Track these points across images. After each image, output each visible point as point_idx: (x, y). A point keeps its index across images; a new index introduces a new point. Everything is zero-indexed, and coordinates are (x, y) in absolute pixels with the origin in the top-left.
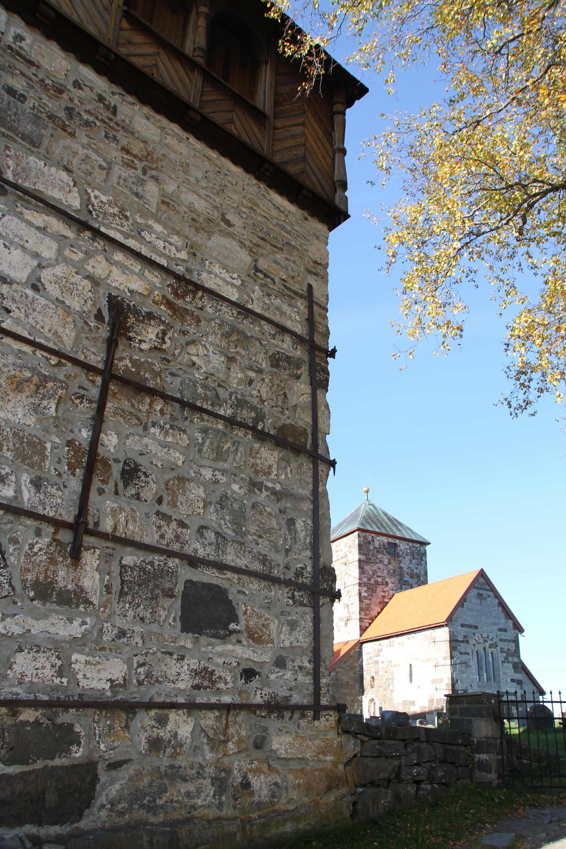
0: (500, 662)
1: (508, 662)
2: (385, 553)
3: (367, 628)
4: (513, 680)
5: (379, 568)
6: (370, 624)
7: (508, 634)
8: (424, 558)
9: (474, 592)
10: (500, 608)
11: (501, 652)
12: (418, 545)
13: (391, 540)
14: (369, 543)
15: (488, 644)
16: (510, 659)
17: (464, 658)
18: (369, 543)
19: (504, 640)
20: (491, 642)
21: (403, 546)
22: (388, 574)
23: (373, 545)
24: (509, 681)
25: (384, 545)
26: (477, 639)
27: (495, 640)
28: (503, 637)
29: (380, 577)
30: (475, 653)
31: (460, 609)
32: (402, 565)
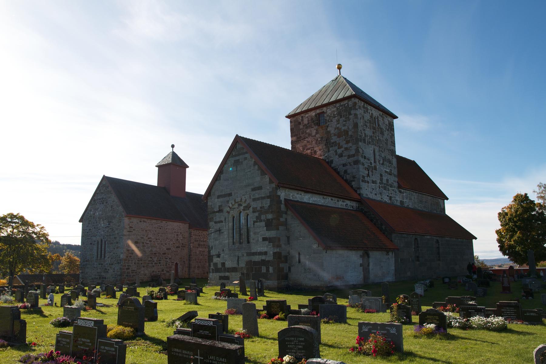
1: (261, 221)
2: (313, 126)
4: (264, 239)
5: (308, 142)
7: (263, 191)
8: (353, 112)
9: (231, 160)
10: (256, 167)
11: (254, 212)
12: (346, 102)
13: (318, 111)
14: (300, 123)
15: (242, 208)
16: (263, 217)
17: (219, 225)
18: (300, 123)
19: (258, 199)
20: (245, 205)
21: (329, 111)
22: (316, 143)
23: (303, 123)
24: (260, 239)
25: (312, 119)
26: (231, 205)
27: (248, 202)
28: (257, 196)
29: (308, 149)
30: (231, 219)
31: (217, 182)
32: (328, 130)
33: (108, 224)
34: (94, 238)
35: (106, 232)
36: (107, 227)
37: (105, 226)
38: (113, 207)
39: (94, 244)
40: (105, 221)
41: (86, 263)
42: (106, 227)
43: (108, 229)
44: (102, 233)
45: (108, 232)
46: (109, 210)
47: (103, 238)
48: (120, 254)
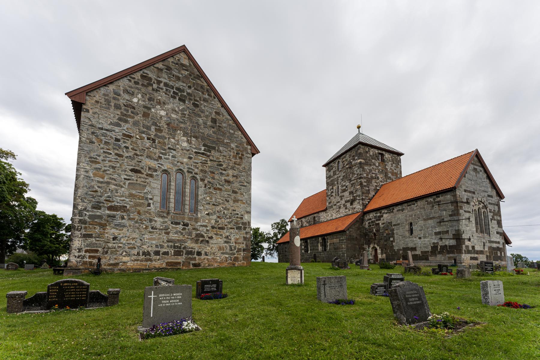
0: (490, 220)
1: (495, 220)
3: (367, 204)
6: (369, 202)
16: (495, 217)
33: (203, 148)
34: (153, 164)
35: (196, 161)
36: (203, 154)
37: (194, 150)
38: (218, 124)
39: (151, 176)
40: (193, 139)
41: (108, 212)
42: (196, 152)
43: (204, 159)
44: (185, 160)
45: (206, 165)
46: (205, 124)
47: (188, 172)
48: (243, 213)
